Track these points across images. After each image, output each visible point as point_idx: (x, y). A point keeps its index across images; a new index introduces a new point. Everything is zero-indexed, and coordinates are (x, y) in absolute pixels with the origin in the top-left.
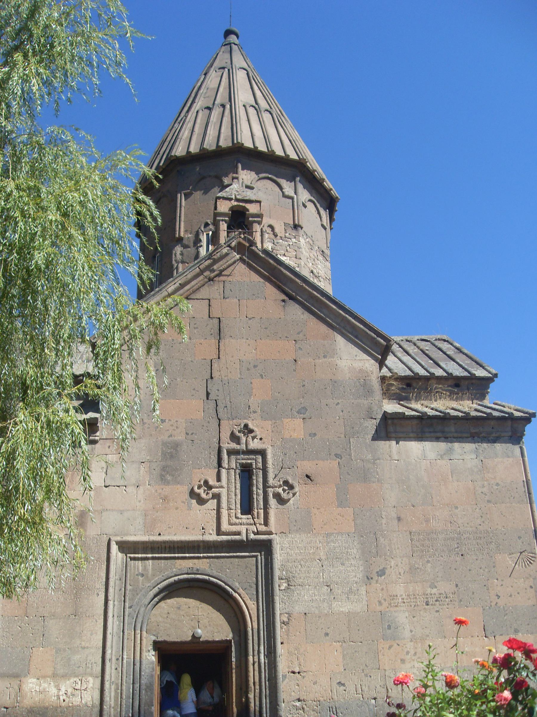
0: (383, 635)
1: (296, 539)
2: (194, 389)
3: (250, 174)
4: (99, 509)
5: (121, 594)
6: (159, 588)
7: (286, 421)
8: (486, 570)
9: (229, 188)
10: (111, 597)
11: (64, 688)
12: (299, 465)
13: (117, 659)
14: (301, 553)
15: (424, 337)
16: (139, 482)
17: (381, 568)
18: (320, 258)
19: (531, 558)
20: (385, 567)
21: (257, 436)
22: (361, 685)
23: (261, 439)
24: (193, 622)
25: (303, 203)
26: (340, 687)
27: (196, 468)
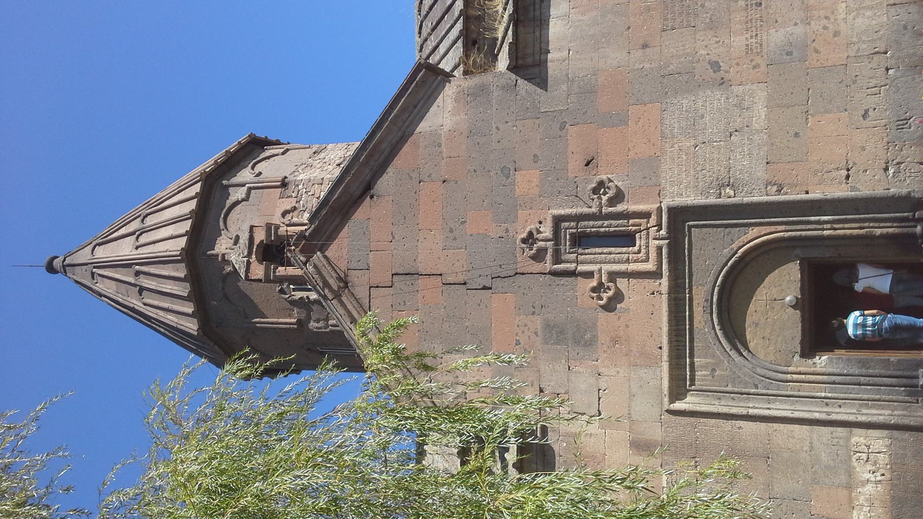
0: (799, 61)
1: (668, 178)
2: (479, 305)
3: (220, 240)
4: (628, 424)
5: (739, 398)
6: (731, 350)
7: (518, 192)
9: (235, 265)
10: (744, 411)
11: (865, 474)
12: (573, 175)
13: (827, 404)
14: (686, 171)
15: (417, 30)
16: (594, 372)
17: (709, 67)
18: (322, 155)
20: (707, 62)
21: (536, 228)
22: (868, 89)
23: (540, 223)
24: (775, 307)
25: (255, 176)
26: (869, 116)
27: (577, 303)
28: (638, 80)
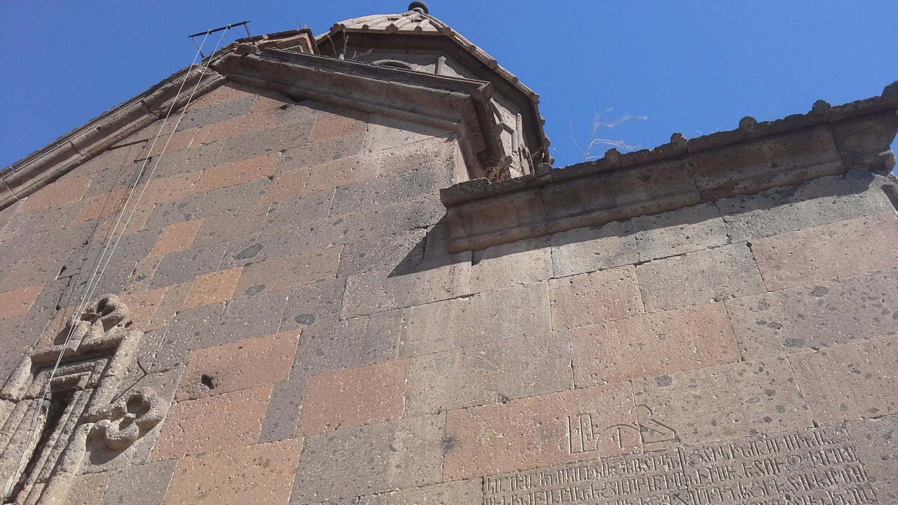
21: (121, 319)
28: (365, 443)
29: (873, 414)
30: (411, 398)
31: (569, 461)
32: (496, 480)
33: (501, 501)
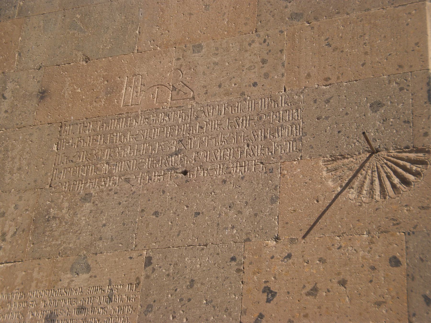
8: (248, 211)
19: (408, 165)
29: (325, 82)
30: (22, 54)
31: (121, 112)
32: (70, 125)
33: (70, 141)
